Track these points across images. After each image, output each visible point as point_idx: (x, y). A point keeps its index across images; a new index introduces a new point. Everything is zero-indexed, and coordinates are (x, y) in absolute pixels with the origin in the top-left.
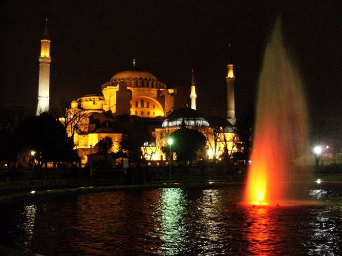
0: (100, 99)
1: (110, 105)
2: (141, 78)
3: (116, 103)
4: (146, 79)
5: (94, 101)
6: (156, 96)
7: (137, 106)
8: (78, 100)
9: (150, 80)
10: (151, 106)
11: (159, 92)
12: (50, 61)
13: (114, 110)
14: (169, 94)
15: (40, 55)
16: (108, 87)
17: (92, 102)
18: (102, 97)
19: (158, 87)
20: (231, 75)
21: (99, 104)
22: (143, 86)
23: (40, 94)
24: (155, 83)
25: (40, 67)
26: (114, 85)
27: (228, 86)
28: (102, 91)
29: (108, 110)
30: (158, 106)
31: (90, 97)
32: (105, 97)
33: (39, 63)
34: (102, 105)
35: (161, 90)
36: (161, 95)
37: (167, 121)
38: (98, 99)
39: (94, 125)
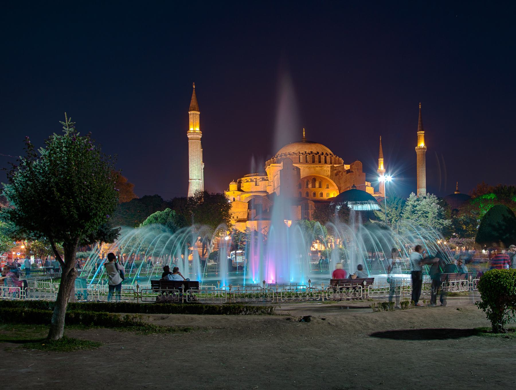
0: (263, 179)
1: (274, 185)
2: (312, 152)
3: (279, 185)
4: (318, 153)
5: (256, 181)
6: (329, 173)
9: (323, 154)
10: (324, 186)
12: (200, 137)
16: (271, 165)
17: (254, 183)
18: (265, 177)
19: (333, 161)
20: (422, 144)
21: (262, 186)
22: (314, 162)
23: (190, 177)
26: (278, 162)
27: (418, 158)
29: (272, 192)
32: (268, 176)
35: (335, 166)
38: (261, 180)
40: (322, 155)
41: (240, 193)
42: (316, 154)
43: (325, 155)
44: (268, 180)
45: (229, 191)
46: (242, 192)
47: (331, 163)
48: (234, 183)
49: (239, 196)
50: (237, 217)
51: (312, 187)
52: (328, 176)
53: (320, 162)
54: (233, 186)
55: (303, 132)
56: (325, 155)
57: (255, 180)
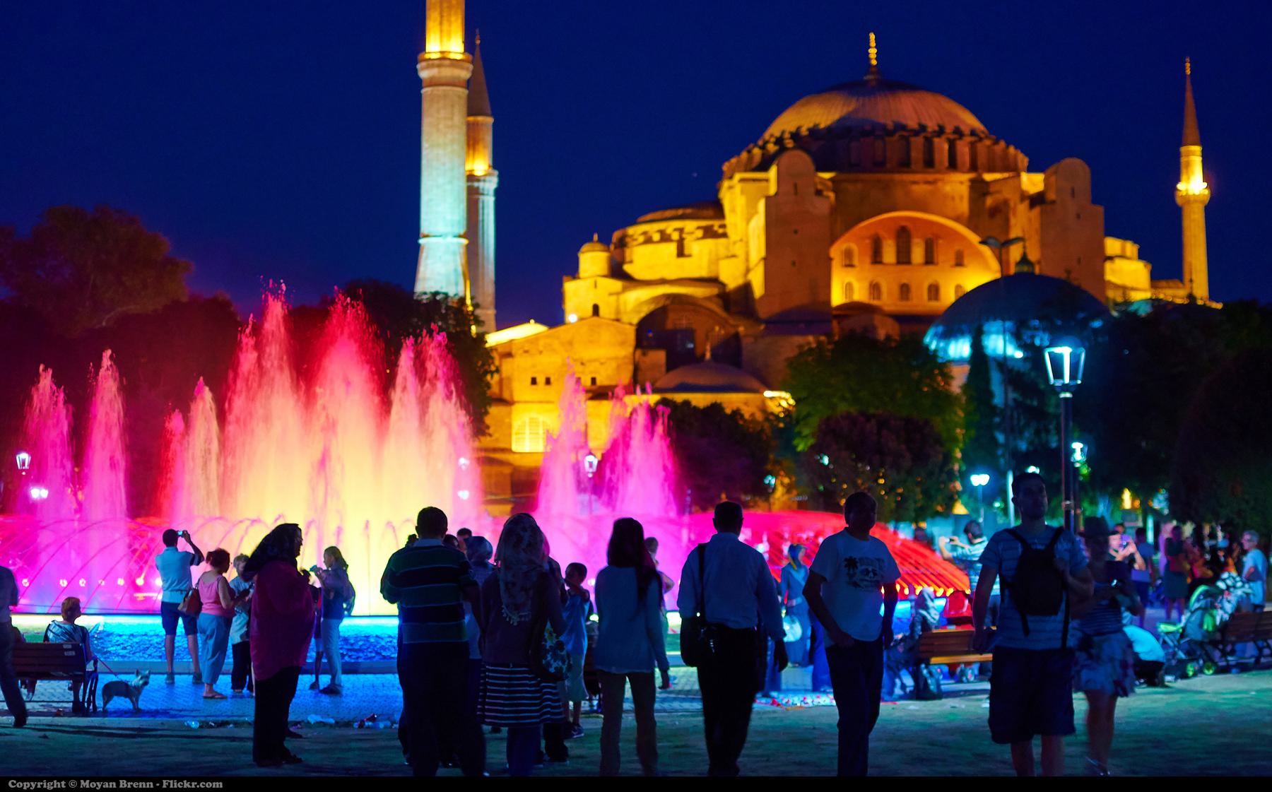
0: (709, 233)
3: (763, 253)
6: (964, 207)
7: (877, 258)
8: (616, 235)
9: (941, 131)
10: (945, 254)
11: (979, 189)
12: (465, 74)
13: (758, 290)
14: (1024, 196)
15: (421, 46)
17: (672, 248)
18: (716, 224)
19: (982, 159)
23: (426, 224)
24: (963, 149)
25: (426, 105)
28: (717, 191)
29: (740, 281)
31: (662, 226)
32: (730, 219)
33: (419, 83)
34: (715, 261)
35: (988, 177)
36: (989, 201)
37: (936, 335)
38: (700, 233)
39: (660, 356)
41: (617, 285)
42: (916, 133)
43: (952, 137)
44: (725, 235)
45: (579, 278)
46: (626, 284)
47: (974, 167)
48: (598, 246)
49: (613, 298)
50: (594, 380)
51: (899, 262)
52: (957, 219)
53: (929, 163)
54: (592, 260)
55: (870, 47)
57: (675, 236)
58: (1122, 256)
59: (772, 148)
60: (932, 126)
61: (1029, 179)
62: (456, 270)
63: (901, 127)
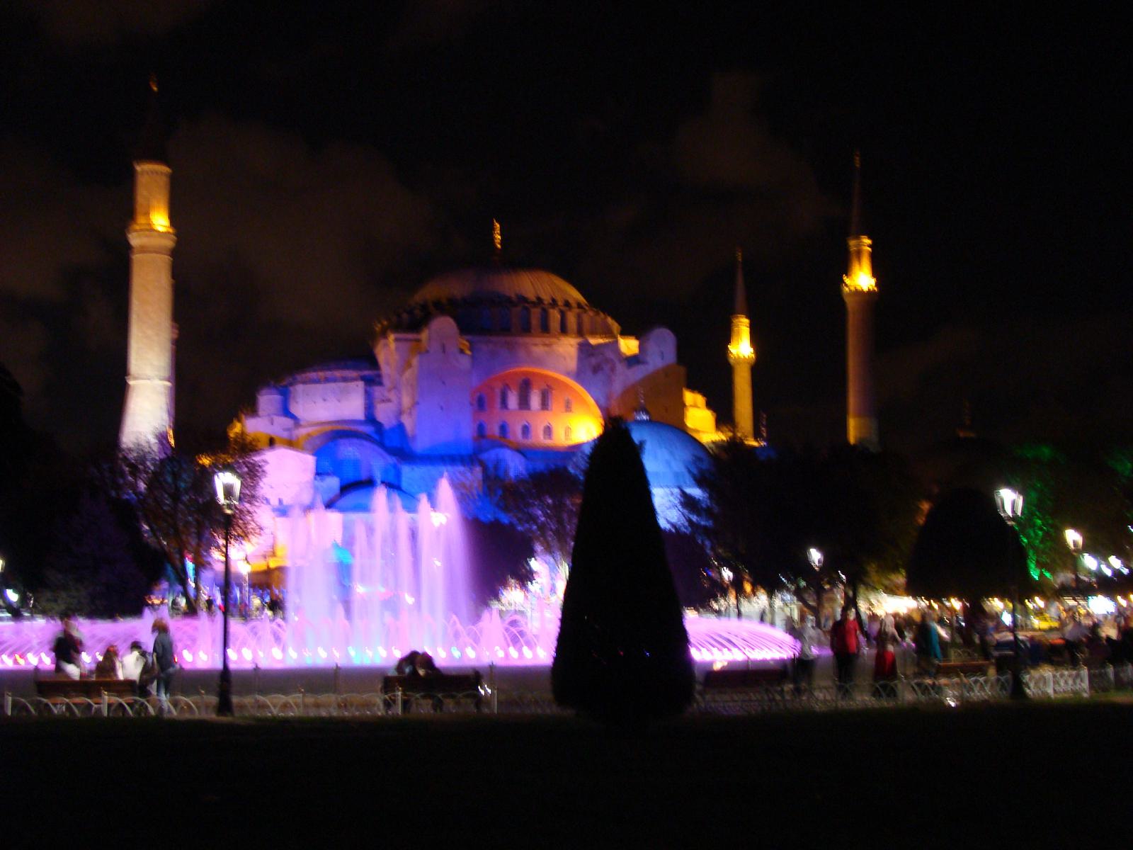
6: (572, 364)
9: (554, 303)
10: (556, 403)
11: (585, 350)
12: (169, 243)
20: (862, 279)
29: (394, 422)
30: (583, 402)
35: (594, 341)
40: (553, 308)
41: (288, 422)
42: (534, 304)
43: (563, 308)
47: (580, 333)
50: (280, 501)
52: (568, 374)
53: (545, 329)
56: (563, 308)
58: (695, 406)
59: (417, 312)
60: (547, 299)
61: (626, 344)
62: (161, 408)
63: (523, 299)
